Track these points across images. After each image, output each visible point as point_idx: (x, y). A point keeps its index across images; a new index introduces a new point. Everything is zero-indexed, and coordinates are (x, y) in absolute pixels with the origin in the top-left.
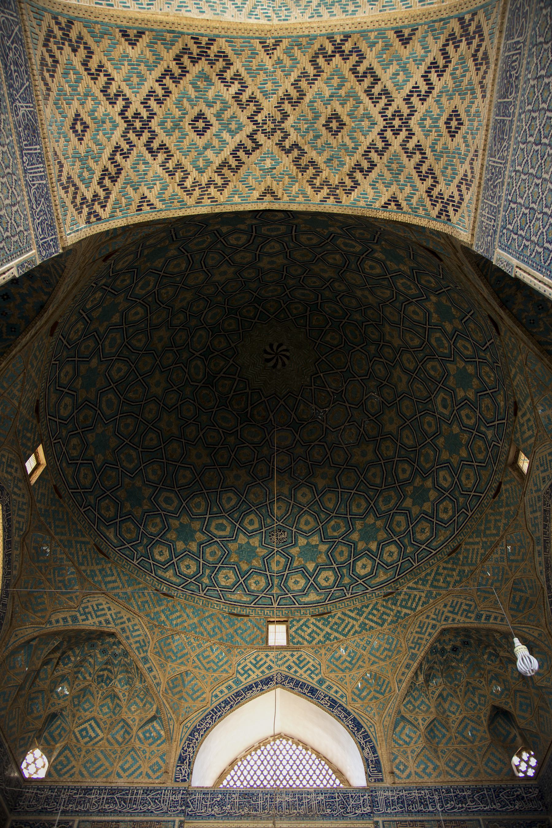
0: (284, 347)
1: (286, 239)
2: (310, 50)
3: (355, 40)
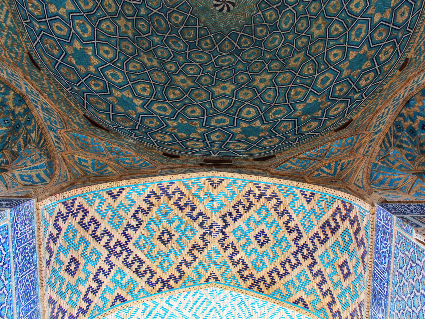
0: (218, 8)
1: (211, 111)
2: (185, 279)
3: (153, 290)
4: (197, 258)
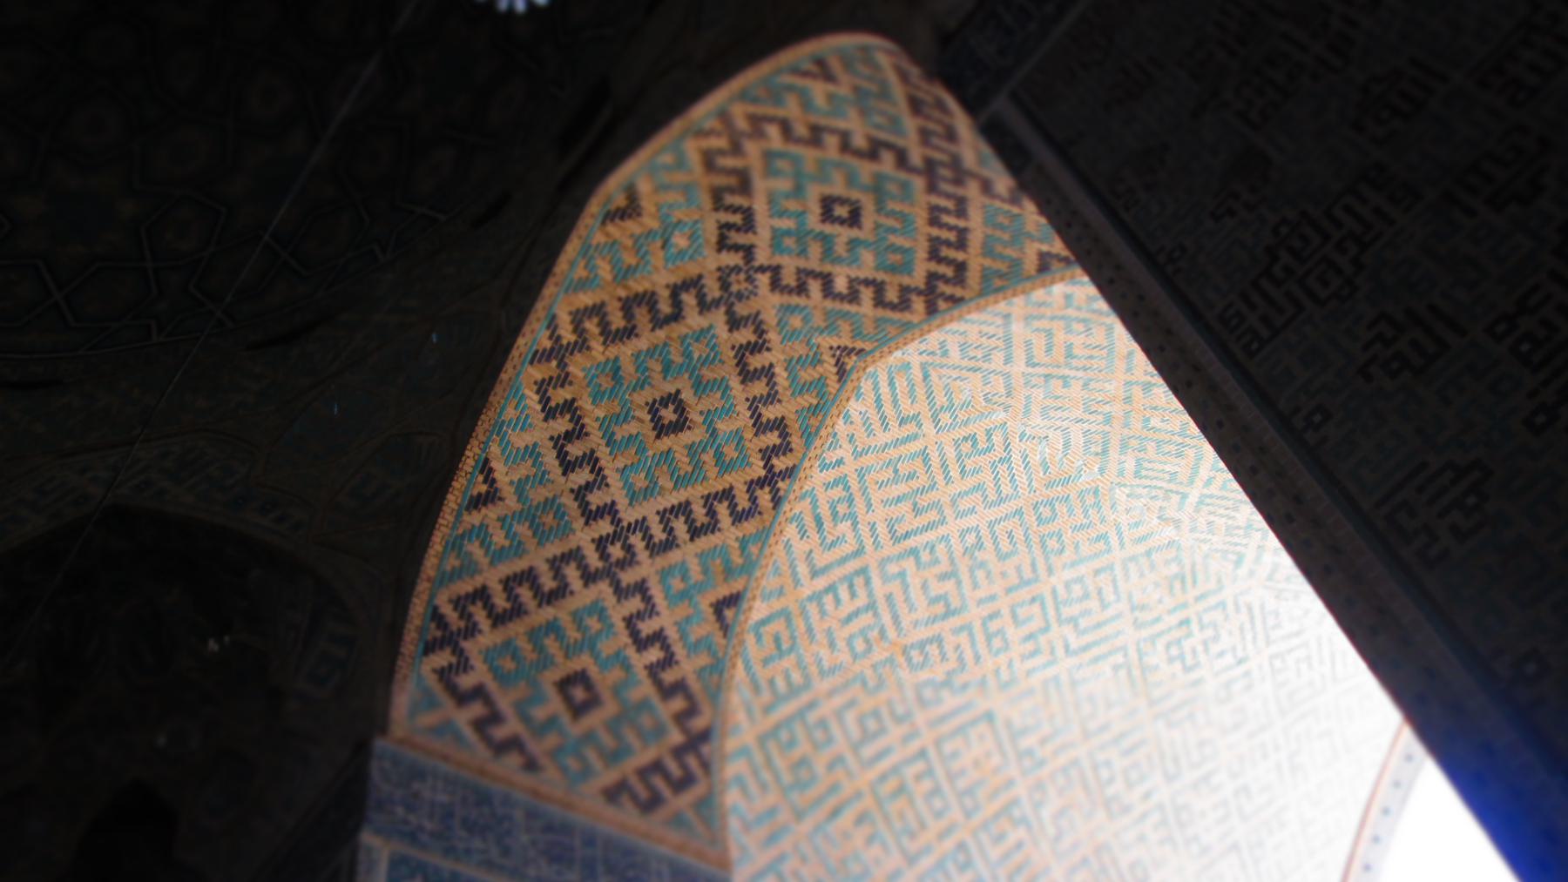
3: (765, 516)
4: (771, 366)
